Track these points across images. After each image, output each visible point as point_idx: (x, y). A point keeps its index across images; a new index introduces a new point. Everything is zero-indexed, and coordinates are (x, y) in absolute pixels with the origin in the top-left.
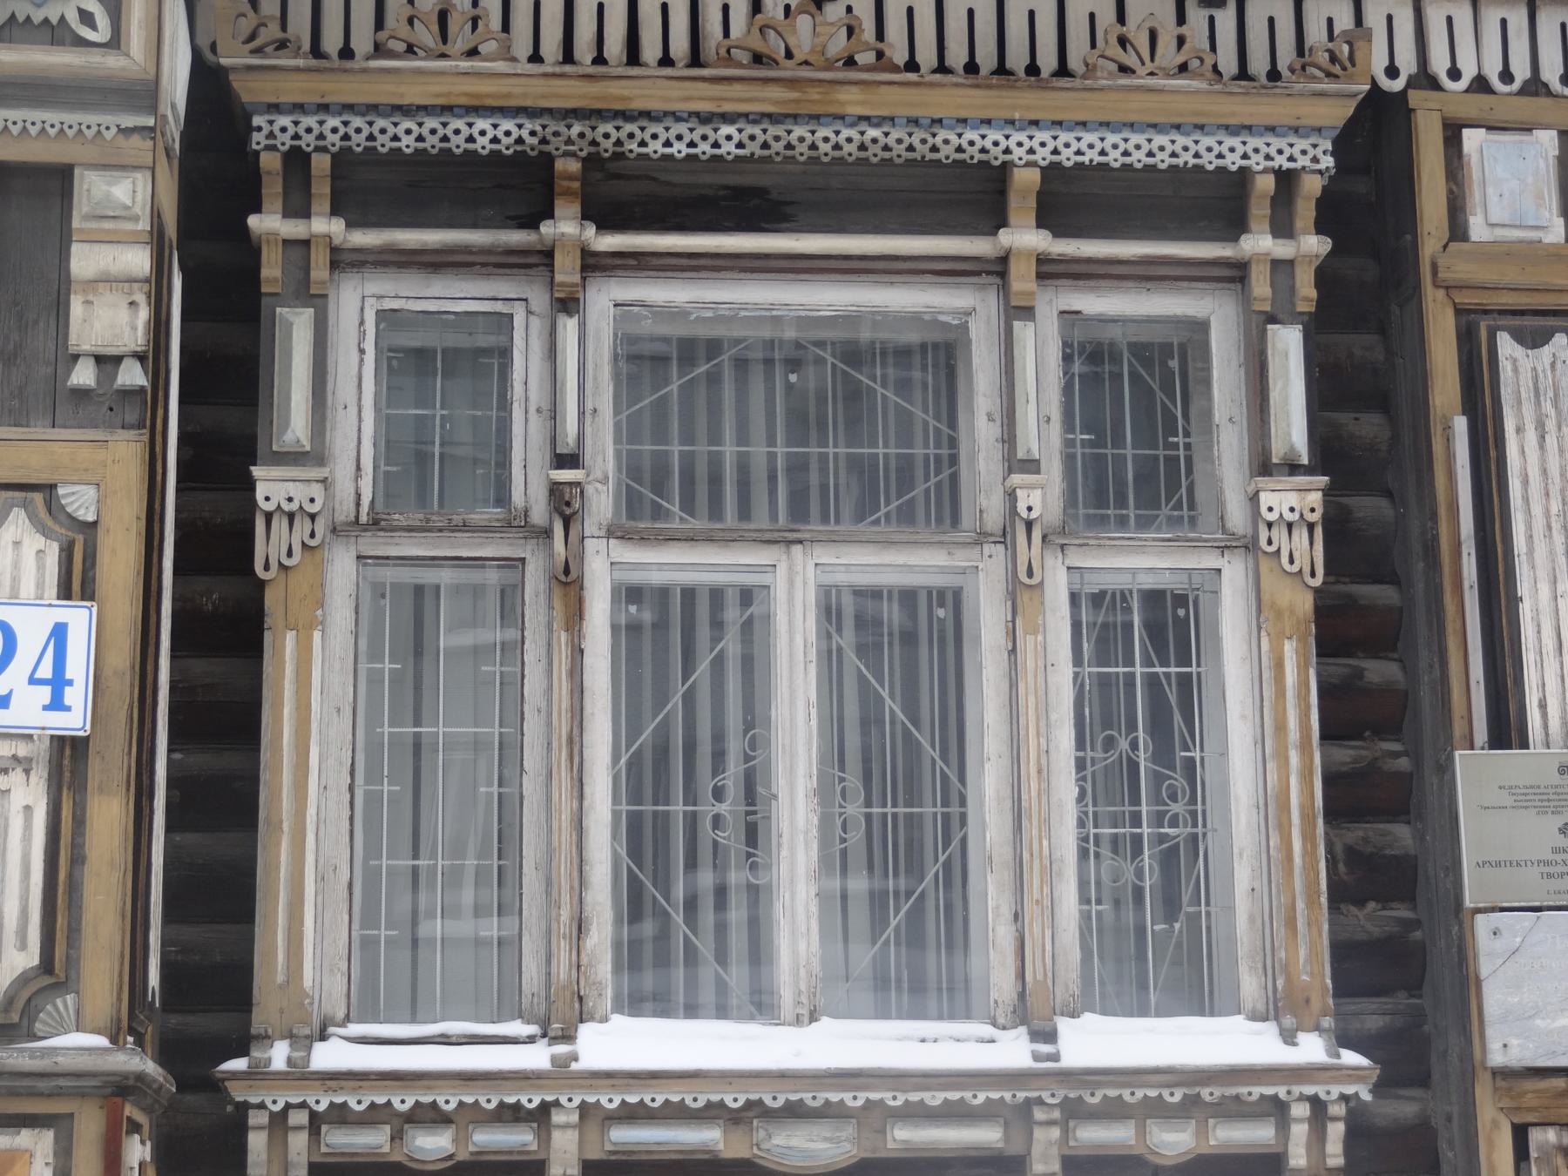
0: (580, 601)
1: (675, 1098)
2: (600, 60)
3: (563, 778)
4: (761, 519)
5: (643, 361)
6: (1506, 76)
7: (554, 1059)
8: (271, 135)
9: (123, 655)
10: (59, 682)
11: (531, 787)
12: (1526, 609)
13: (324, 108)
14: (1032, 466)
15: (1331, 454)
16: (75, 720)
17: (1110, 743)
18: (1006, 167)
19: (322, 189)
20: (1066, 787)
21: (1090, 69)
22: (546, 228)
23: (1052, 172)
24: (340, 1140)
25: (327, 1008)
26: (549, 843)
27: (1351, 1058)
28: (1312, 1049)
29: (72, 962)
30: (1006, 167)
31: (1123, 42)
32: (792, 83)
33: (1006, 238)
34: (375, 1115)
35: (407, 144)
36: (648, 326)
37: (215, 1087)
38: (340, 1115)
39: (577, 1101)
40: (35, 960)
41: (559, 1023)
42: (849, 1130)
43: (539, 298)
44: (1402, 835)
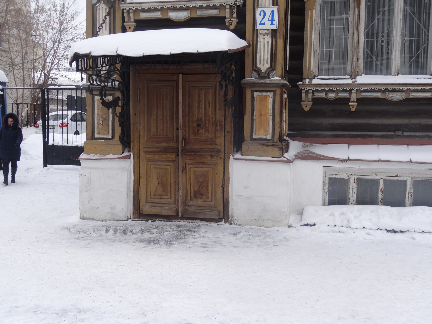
0: (360, 2)
1: (373, 88)
3: (356, 34)
7: (352, 82)
9: (283, 16)
10: (273, 20)
11: (350, 36)
16: (275, 27)
24: (317, 95)
25: (315, 74)
26: (353, 45)
29: (275, 66)
34: (322, 91)
37: (297, 86)
38: (317, 91)
39: (356, 89)
40: (269, 65)
41: (353, 76)
42: (403, 93)
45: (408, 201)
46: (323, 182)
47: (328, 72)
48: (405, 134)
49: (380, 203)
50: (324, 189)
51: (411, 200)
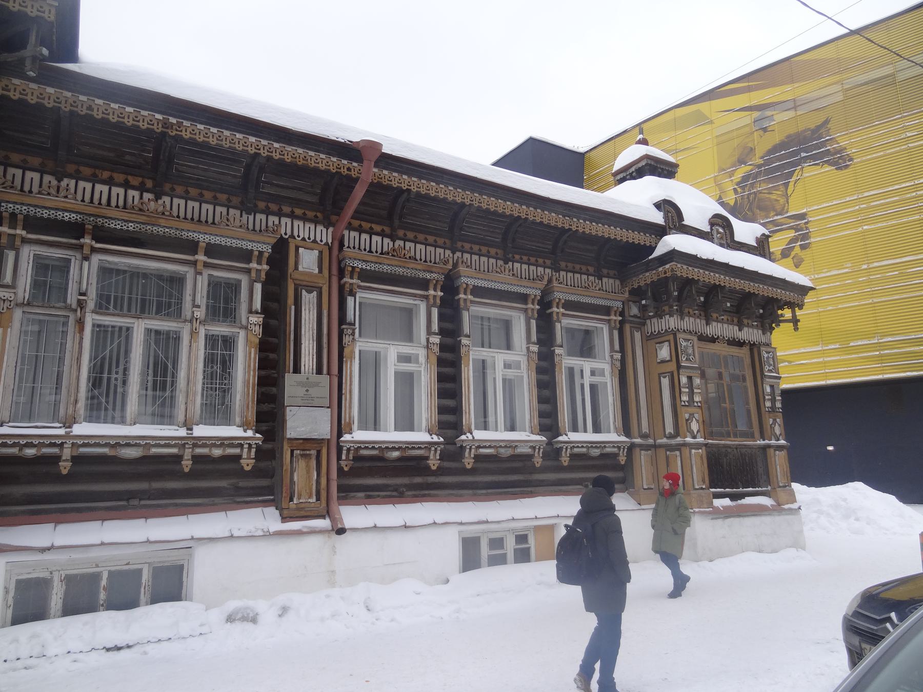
2: (100, 204)
4: (133, 312)
5: (105, 271)
6: (309, 238)
11: (66, 369)
12: (303, 346)
13: (23, 204)
14: (198, 307)
15: (265, 310)
17: (212, 367)
18: (198, 242)
19: (20, 223)
20: (200, 377)
21: (219, 224)
22: (82, 240)
23: (208, 244)
25: (4, 419)
27: (258, 435)
28: (250, 433)
30: (198, 242)
31: (228, 220)
32: (148, 216)
33: (197, 257)
34: (14, 445)
35: (45, 216)
36: (107, 265)
41: (69, 423)
42: (141, 449)
43: (79, 256)
44: (274, 390)
45: (143, 598)
46: (5, 588)
47: (29, 416)
48: (143, 502)
49: (101, 608)
50: (5, 599)
51: (148, 596)
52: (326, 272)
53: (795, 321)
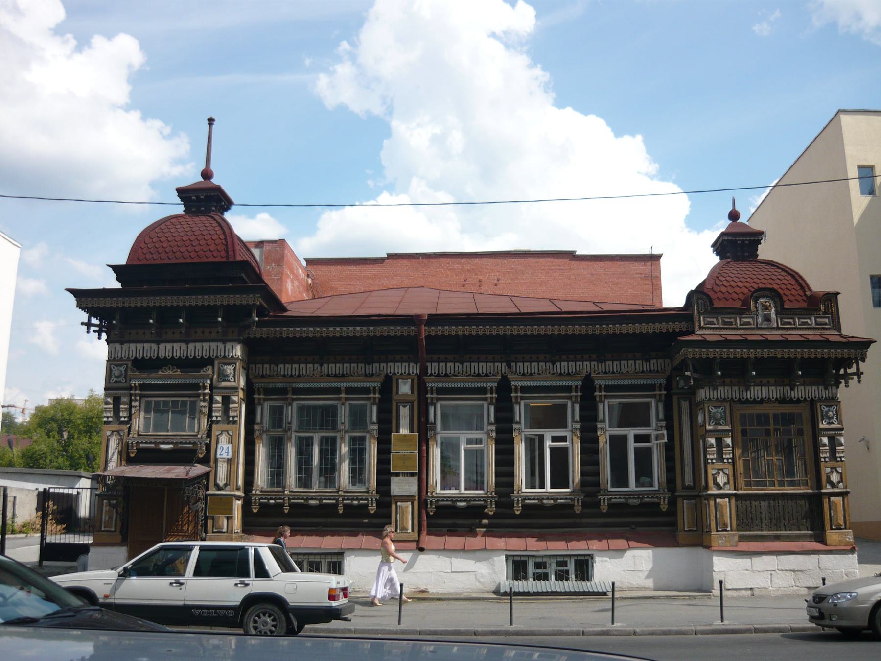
5: (301, 409)
8: (256, 386)
52: (416, 392)
53: (859, 374)
